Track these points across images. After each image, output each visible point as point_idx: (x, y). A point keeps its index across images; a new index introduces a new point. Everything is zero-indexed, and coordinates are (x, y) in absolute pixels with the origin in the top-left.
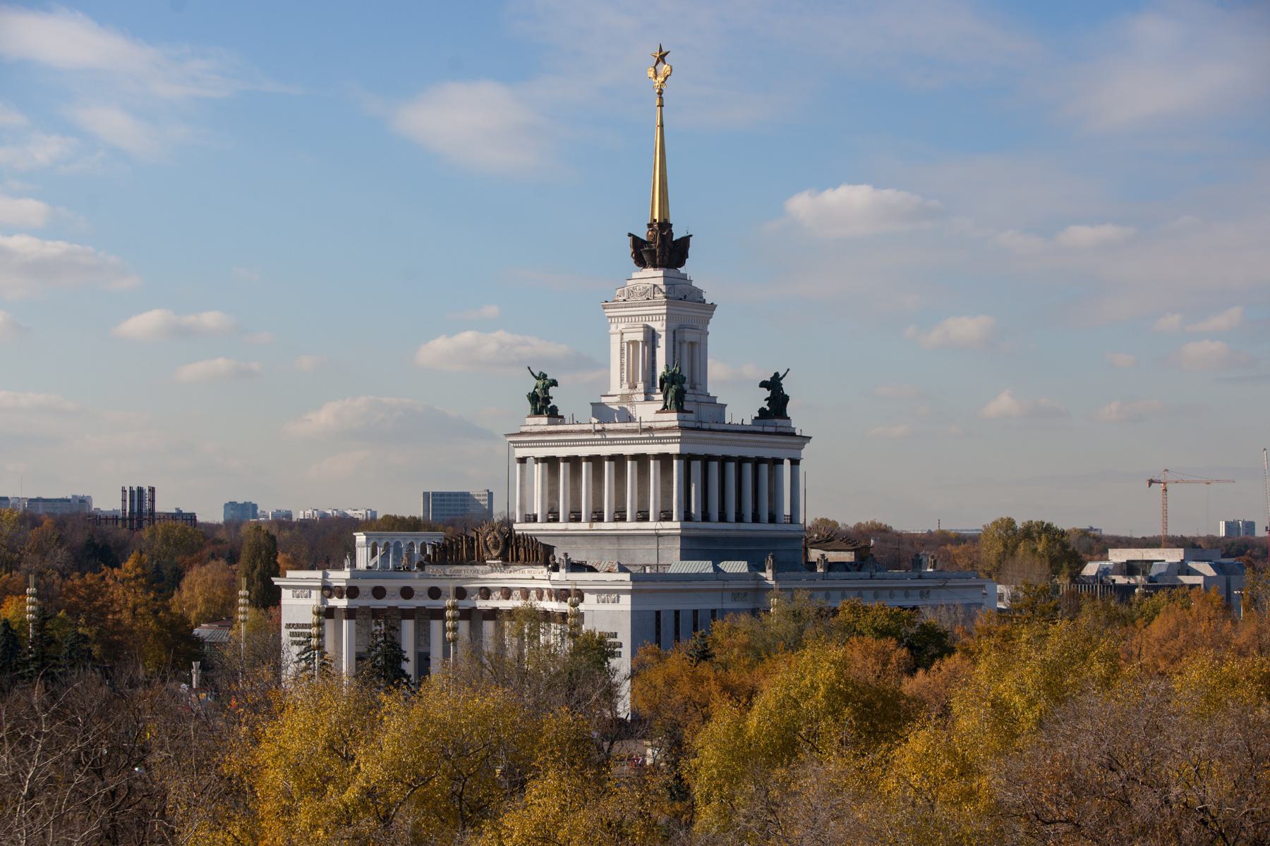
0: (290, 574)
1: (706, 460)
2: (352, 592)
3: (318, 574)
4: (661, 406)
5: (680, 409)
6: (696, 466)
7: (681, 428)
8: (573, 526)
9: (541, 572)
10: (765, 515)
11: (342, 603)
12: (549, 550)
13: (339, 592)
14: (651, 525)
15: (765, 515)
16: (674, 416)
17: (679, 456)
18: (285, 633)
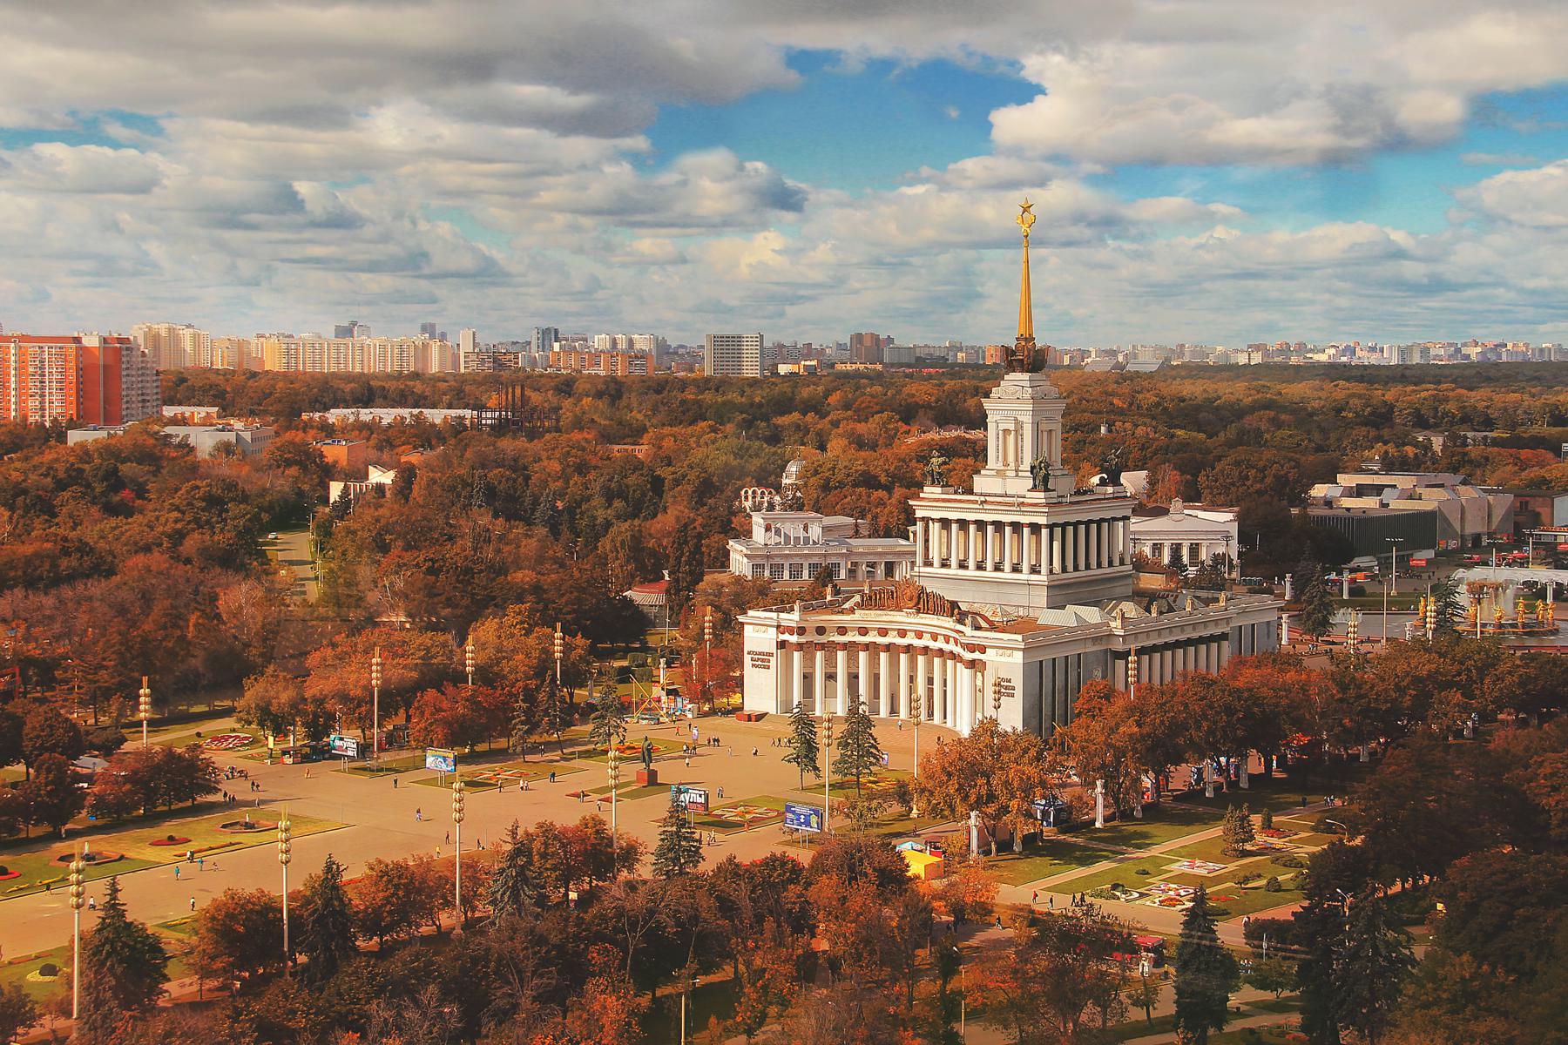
0: (750, 613)
1: (1064, 526)
2: (801, 631)
3: (774, 615)
4: (1030, 483)
5: (1047, 490)
6: (1058, 530)
7: (1048, 505)
8: (962, 572)
9: (948, 622)
10: (1105, 563)
11: (794, 639)
12: (954, 605)
13: (790, 631)
14: (1024, 576)
15: (1105, 563)
16: (1042, 495)
17: (1047, 526)
18: (747, 659)
